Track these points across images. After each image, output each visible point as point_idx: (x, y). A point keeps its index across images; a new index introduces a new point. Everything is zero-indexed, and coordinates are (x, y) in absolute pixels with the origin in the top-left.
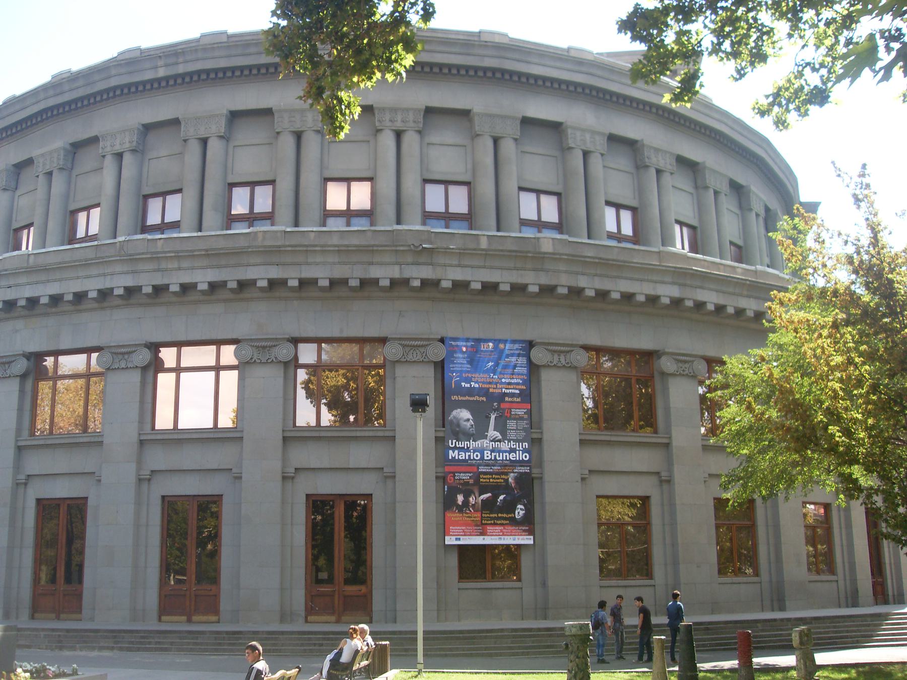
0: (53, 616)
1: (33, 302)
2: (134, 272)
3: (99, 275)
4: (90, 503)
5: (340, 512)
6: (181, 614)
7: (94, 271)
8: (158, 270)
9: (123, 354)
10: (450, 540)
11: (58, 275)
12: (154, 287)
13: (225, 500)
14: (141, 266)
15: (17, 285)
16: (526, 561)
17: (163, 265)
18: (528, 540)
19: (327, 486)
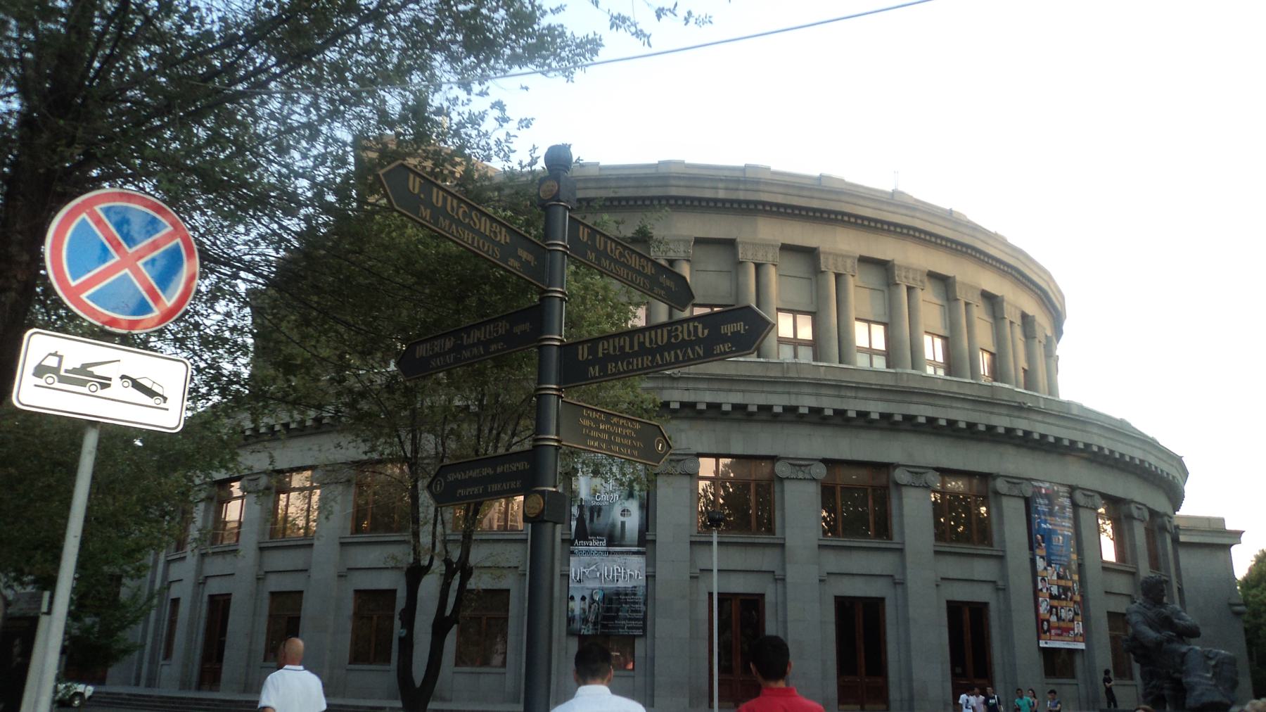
0: (732, 704)
1: (714, 407)
2: (817, 395)
3: (783, 393)
4: (767, 599)
5: (966, 616)
6: (855, 703)
7: (780, 389)
8: (838, 396)
9: (800, 466)
10: (1042, 644)
11: (742, 387)
12: (835, 411)
13: (887, 602)
14: (824, 391)
15: (694, 389)
16: (1078, 661)
17: (843, 393)
18: (1082, 646)
19: (963, 594)
